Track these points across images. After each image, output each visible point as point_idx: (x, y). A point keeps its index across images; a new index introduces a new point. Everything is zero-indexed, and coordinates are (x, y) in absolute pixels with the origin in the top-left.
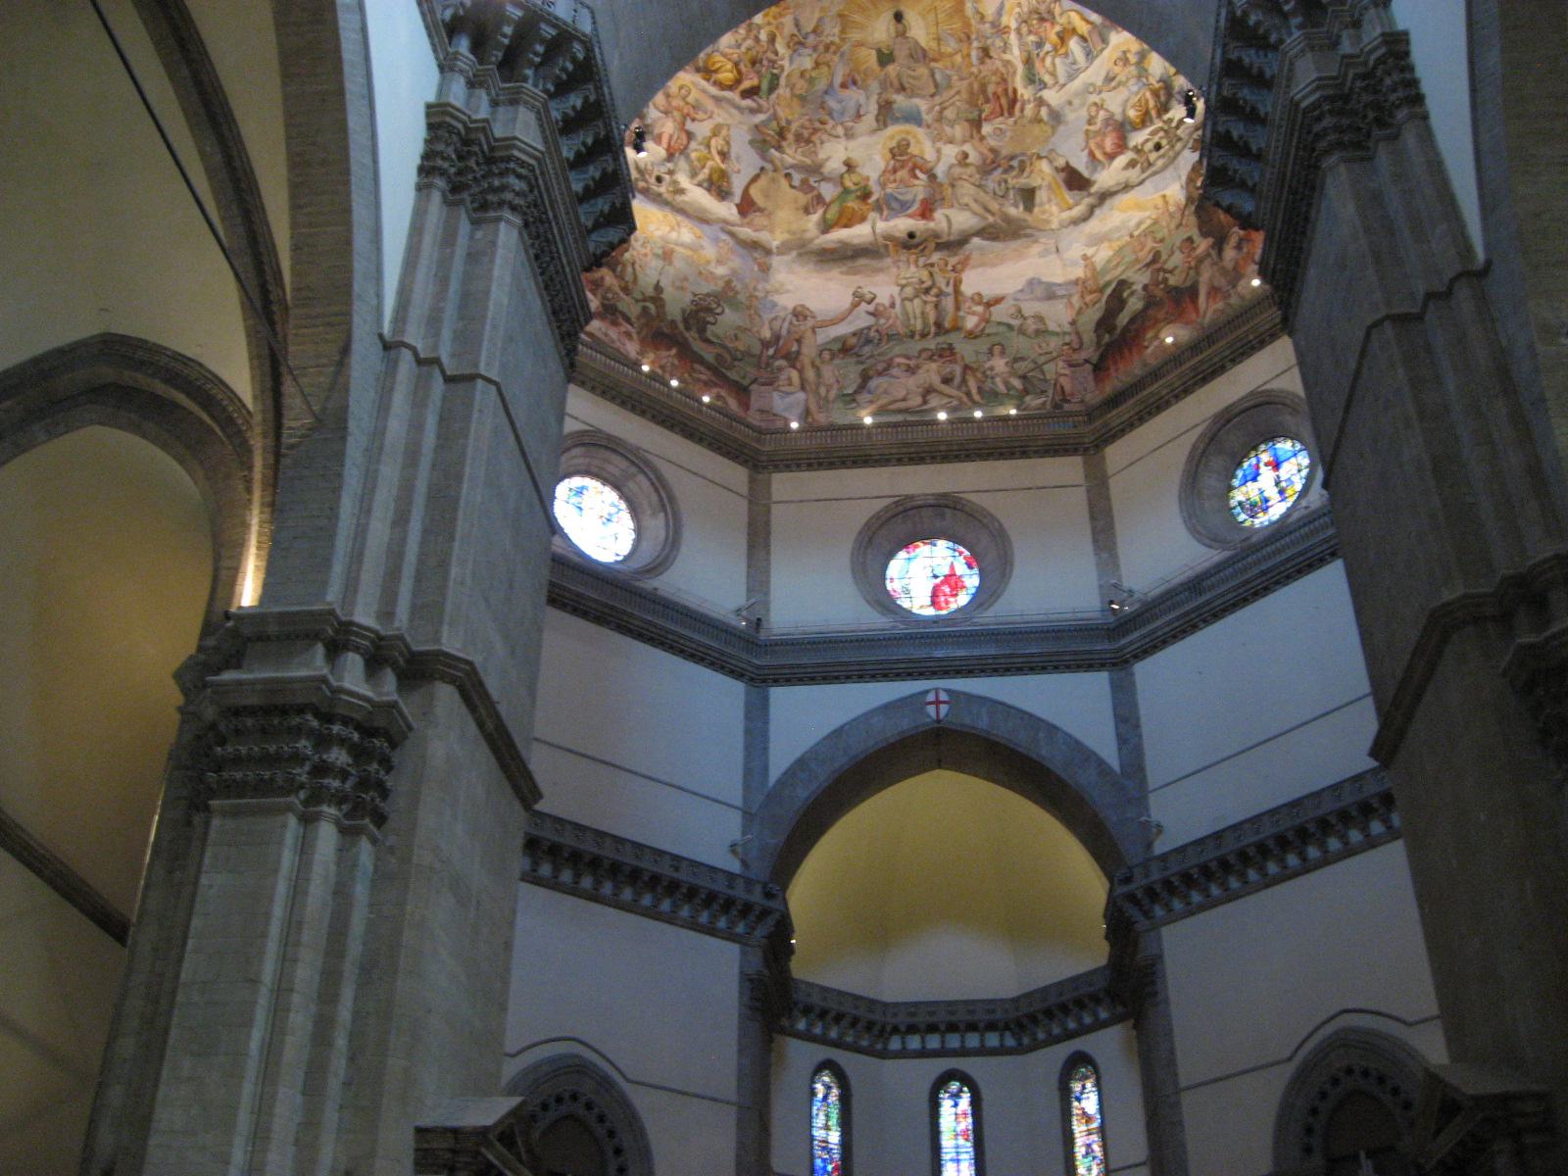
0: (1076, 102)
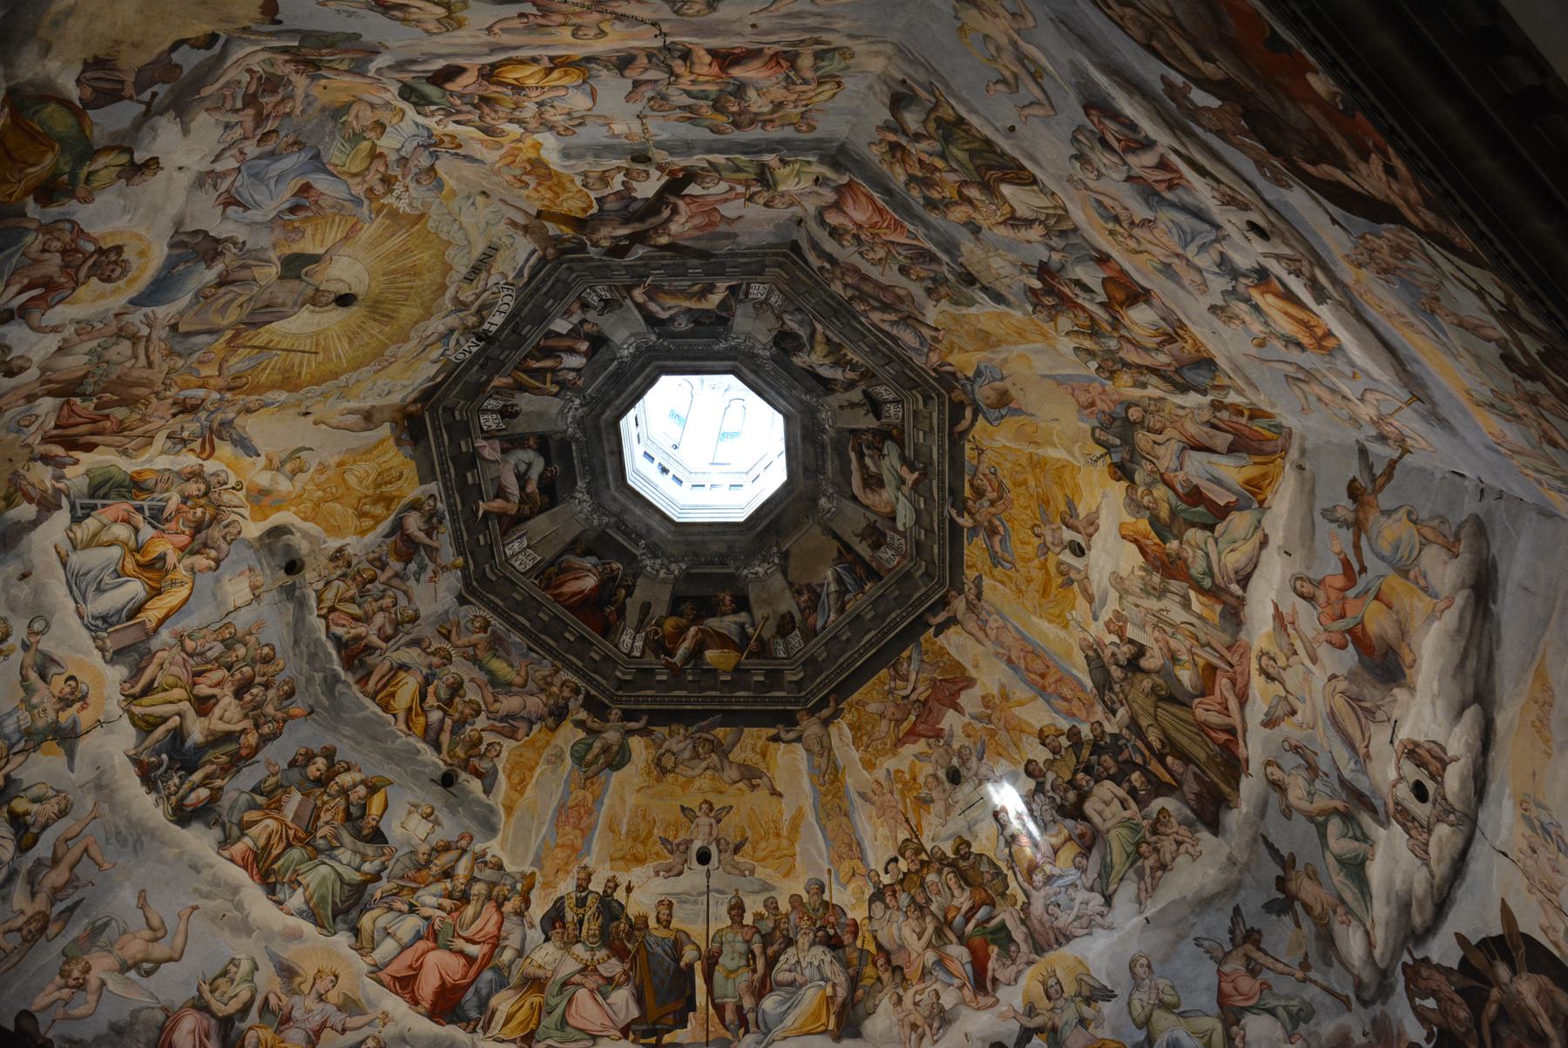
0: (23, 591)
